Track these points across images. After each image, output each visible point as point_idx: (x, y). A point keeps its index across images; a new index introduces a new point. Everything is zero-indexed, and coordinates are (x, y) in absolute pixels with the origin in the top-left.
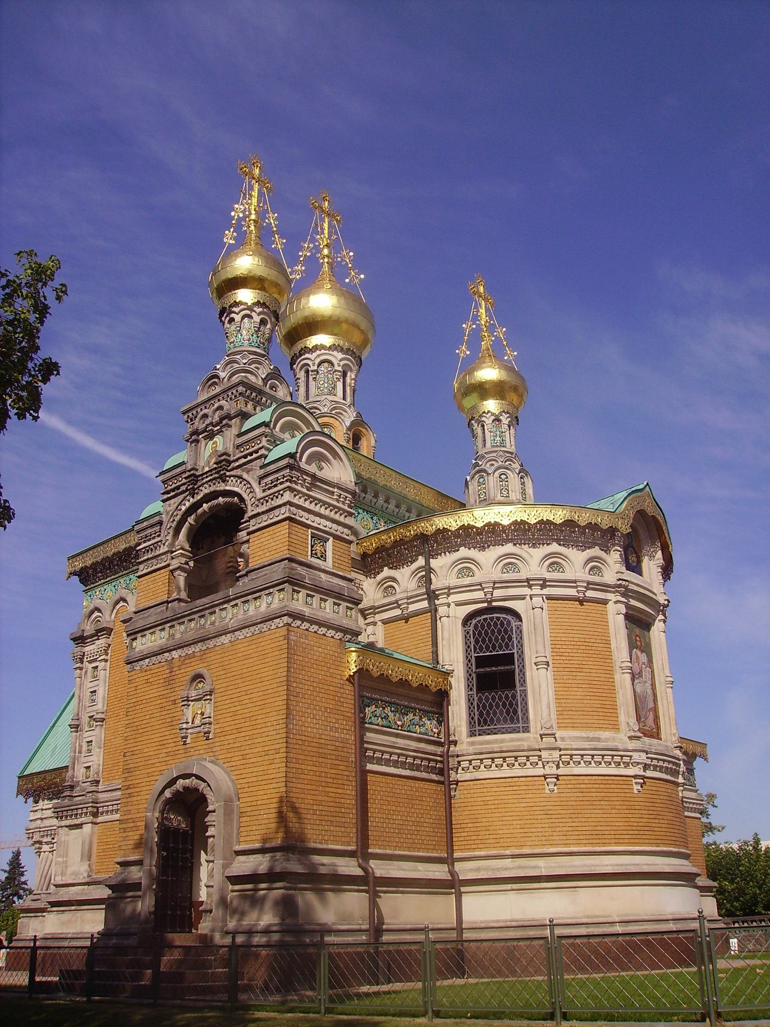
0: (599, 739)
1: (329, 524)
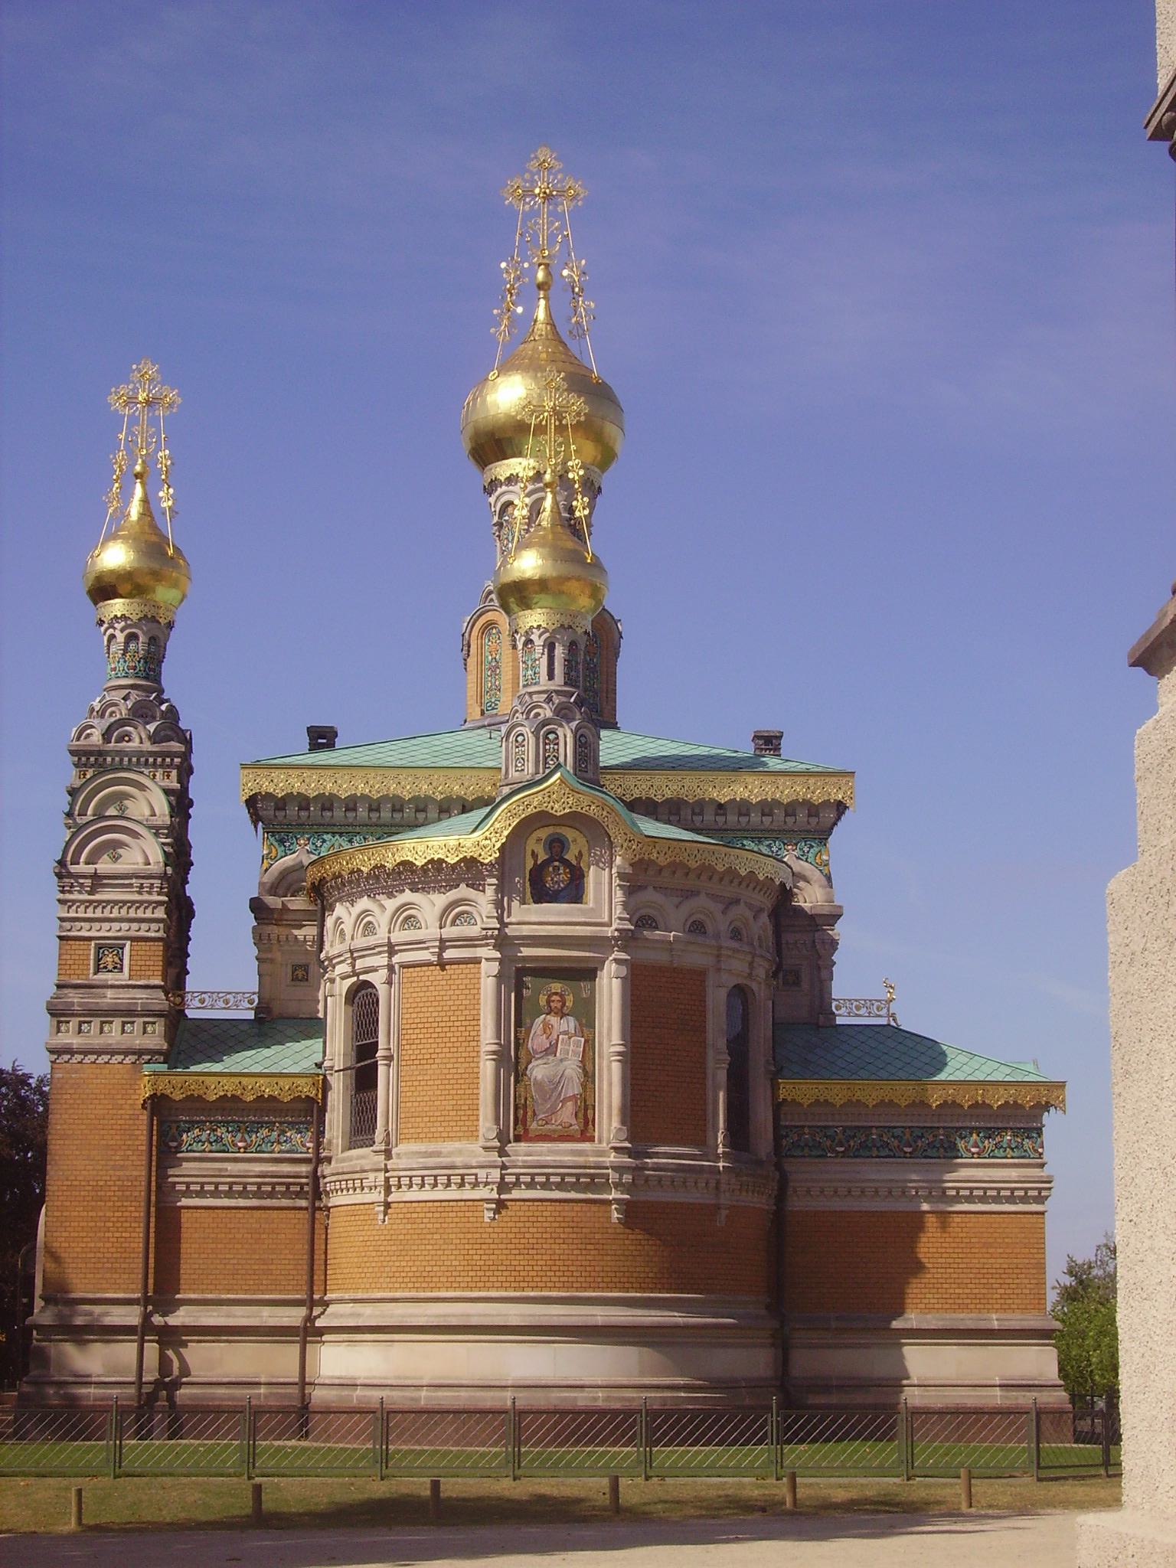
0: (438, 1154)
1: (125, 926)
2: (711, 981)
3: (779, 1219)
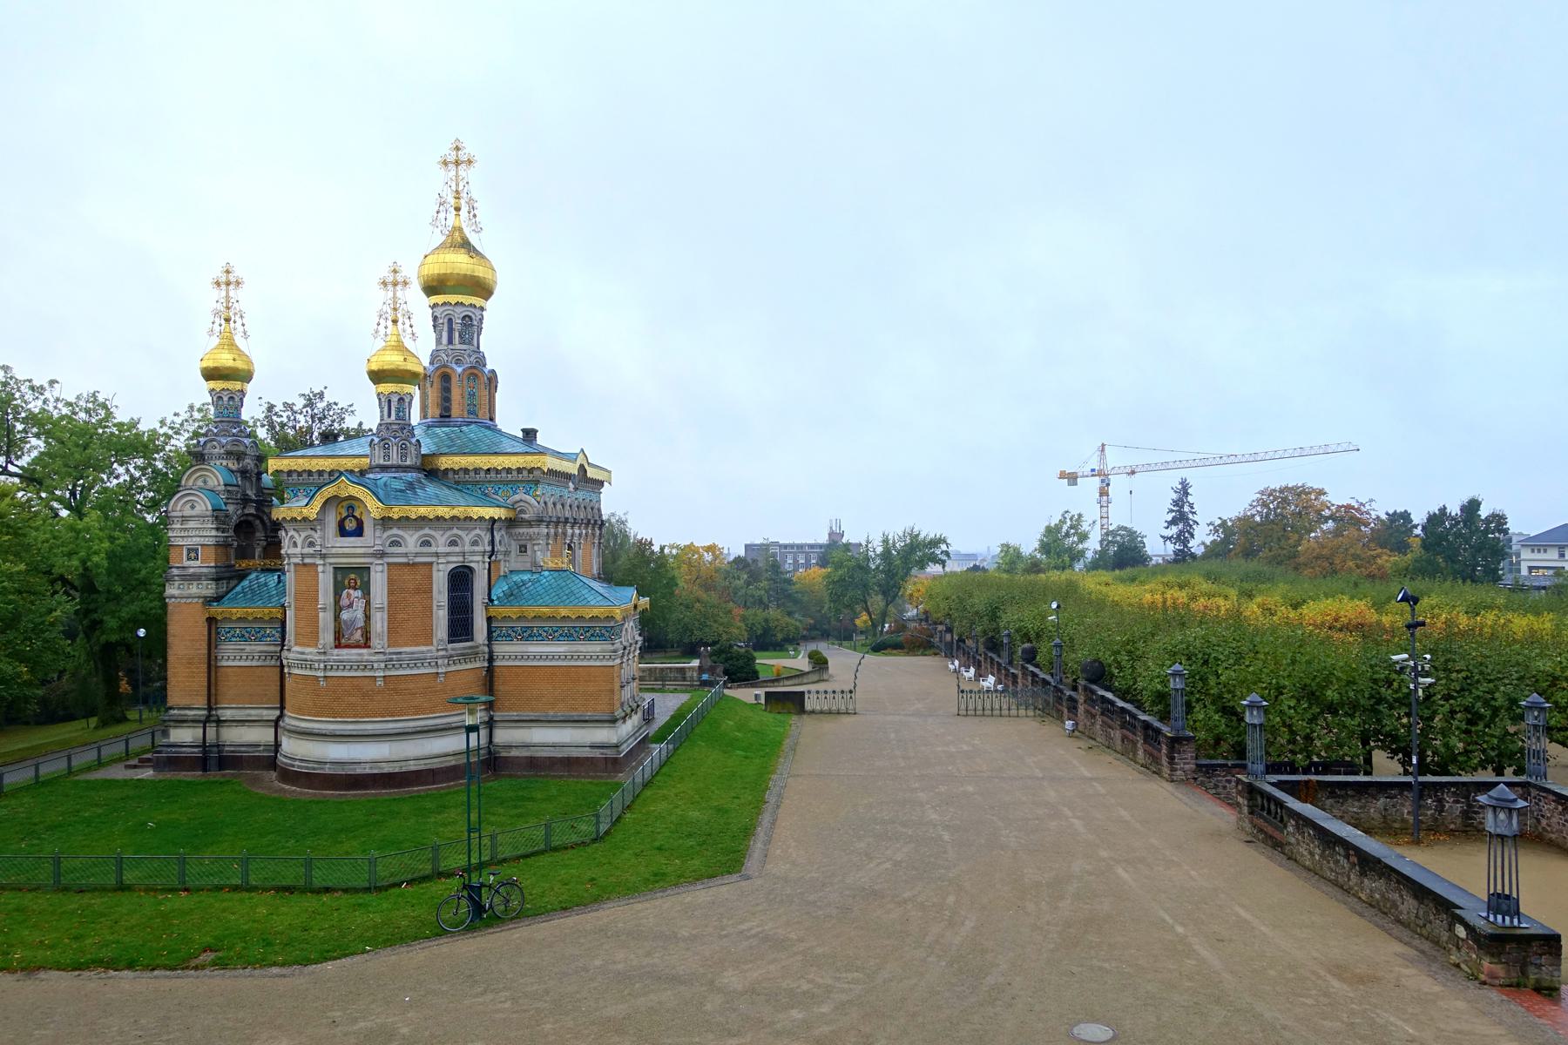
2: (435, 567)
3: (490, 670)
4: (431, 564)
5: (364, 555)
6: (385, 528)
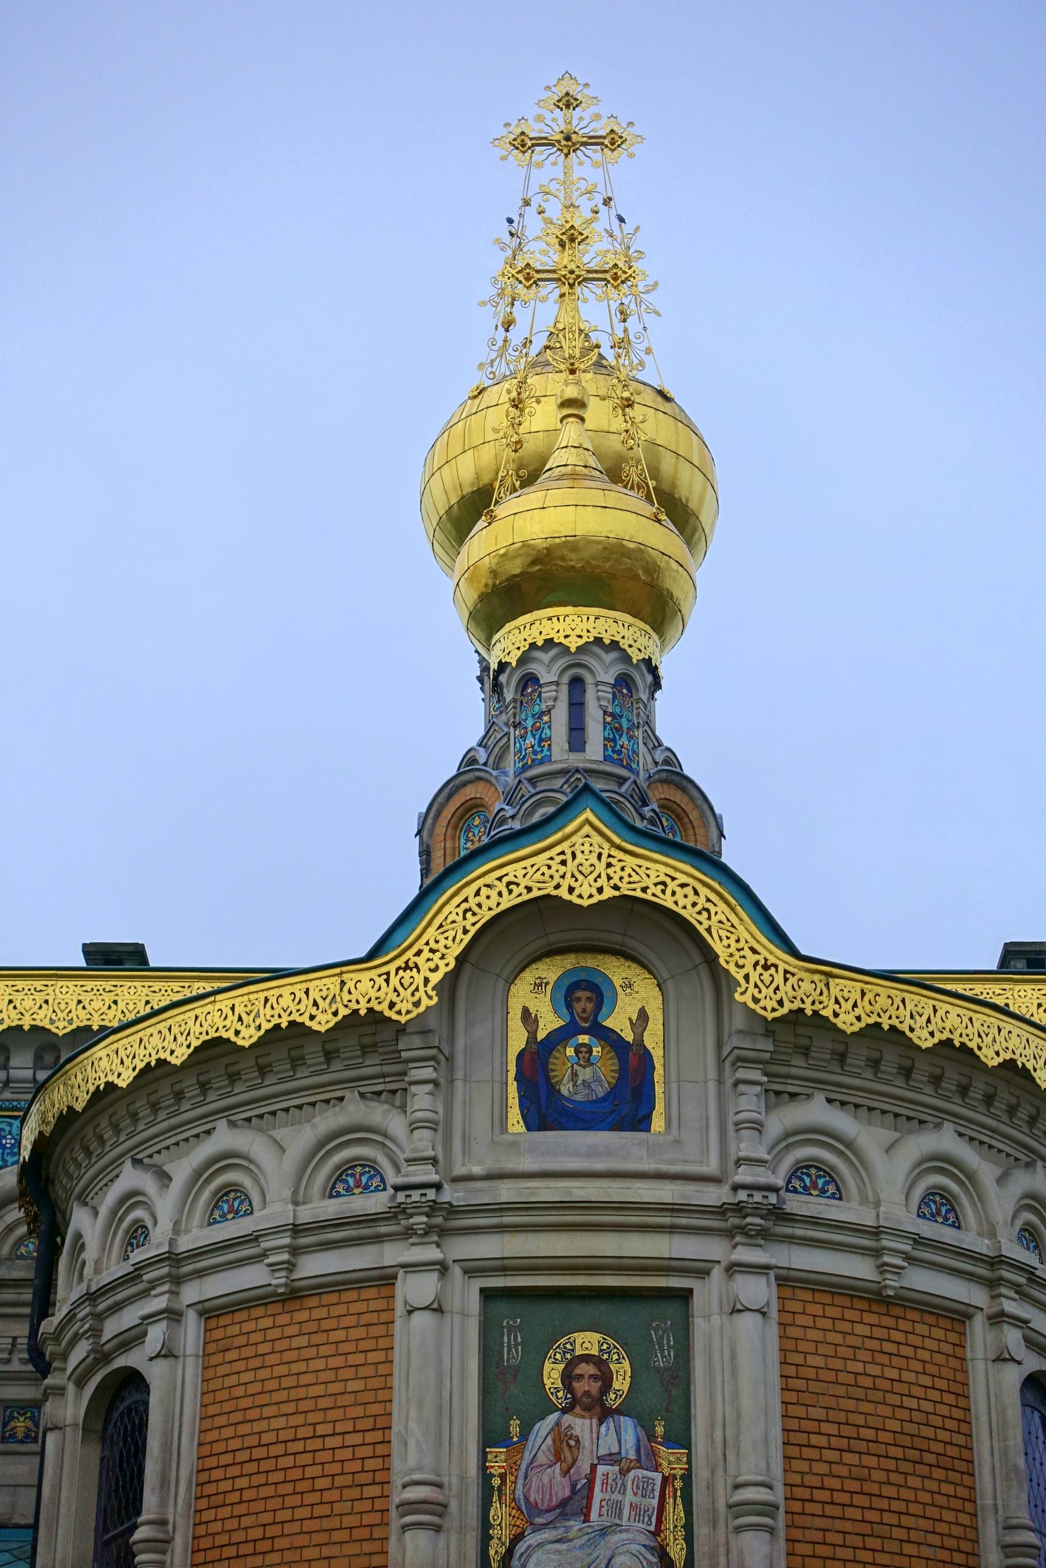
2: (980, 1337)
4: (958, 1316)
5: (672, 1219)
6: (777, 1096)
